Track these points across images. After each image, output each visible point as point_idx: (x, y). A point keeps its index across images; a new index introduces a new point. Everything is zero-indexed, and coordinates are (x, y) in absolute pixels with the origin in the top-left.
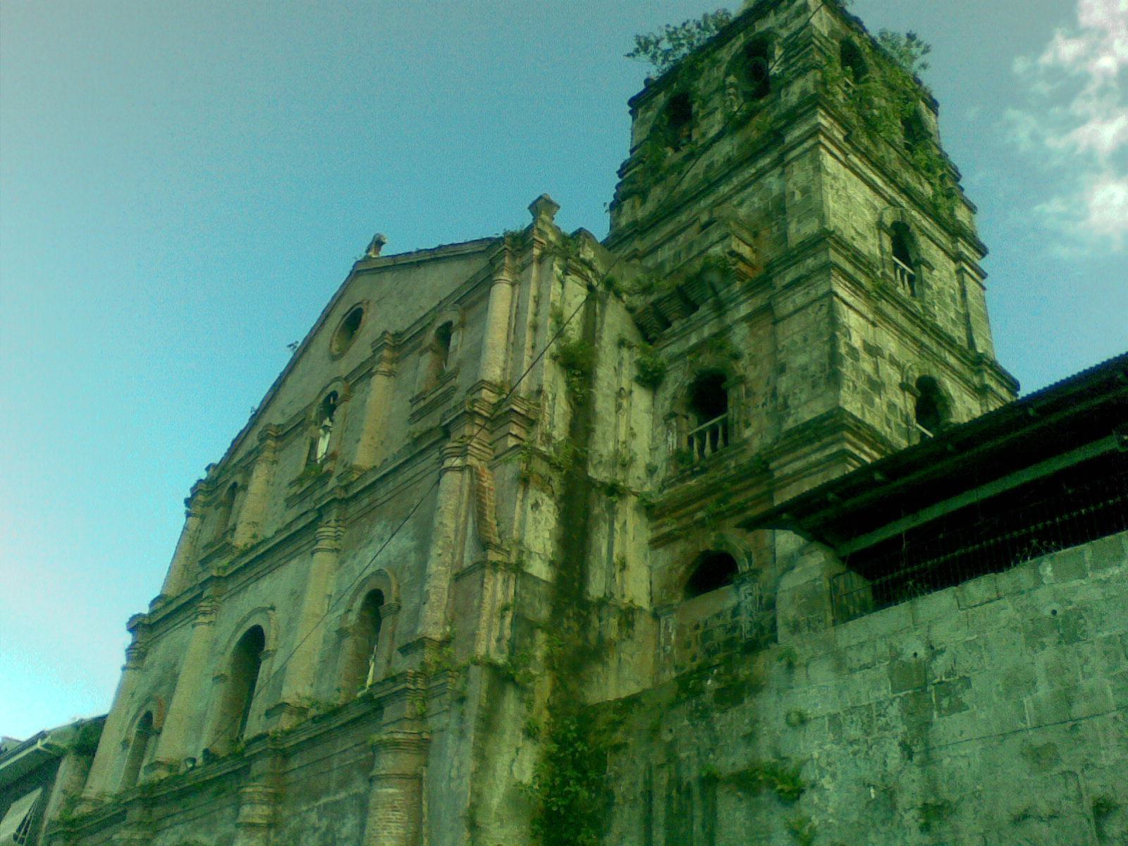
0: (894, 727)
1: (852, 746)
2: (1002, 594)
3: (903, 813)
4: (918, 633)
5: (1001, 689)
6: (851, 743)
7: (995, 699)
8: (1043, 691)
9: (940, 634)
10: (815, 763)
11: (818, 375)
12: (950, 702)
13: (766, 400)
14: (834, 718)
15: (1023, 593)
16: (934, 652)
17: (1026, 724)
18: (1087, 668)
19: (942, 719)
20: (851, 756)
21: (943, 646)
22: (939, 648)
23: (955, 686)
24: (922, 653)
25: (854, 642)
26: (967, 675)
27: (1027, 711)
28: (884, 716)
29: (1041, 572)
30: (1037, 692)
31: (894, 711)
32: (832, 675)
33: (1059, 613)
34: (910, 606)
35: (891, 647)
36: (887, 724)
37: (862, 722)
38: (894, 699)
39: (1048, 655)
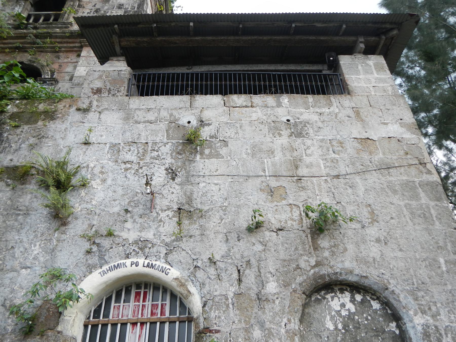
0: (164, 159)
1: (125, 164)
2: (254, 105)
3: (160, 212)
4: (193, 112)
5: (249, 151)
6: (125, 163)
7: (245, 156)
8: (279, 156)
9: (207, 115)
10: (90, 169)
11: (129, 9)
12: (211, 152)
13: (91, 12)
14: (113, 146)
15: (268, 107)
16: (202, 123)
17: (265, 173)
18: (309, 152)
19: (203, 161)
20: (123, 171)
21: (210, 122)
22: (207, 122)
23: (215, 144)
24: (194, 123)
25: (144, 107)
26: (225, 140)
27: (266, 166)
28: (157, 151)
29: (281, 100)
30: (274, 157)
31: (166, 150)
32: (121, 121)
33: (292, 121)
34: (190, 98)
35: (171, 115)
36: (158, 156)
37: (138, 150)
38: (167, 143)
39: (284, 140)
